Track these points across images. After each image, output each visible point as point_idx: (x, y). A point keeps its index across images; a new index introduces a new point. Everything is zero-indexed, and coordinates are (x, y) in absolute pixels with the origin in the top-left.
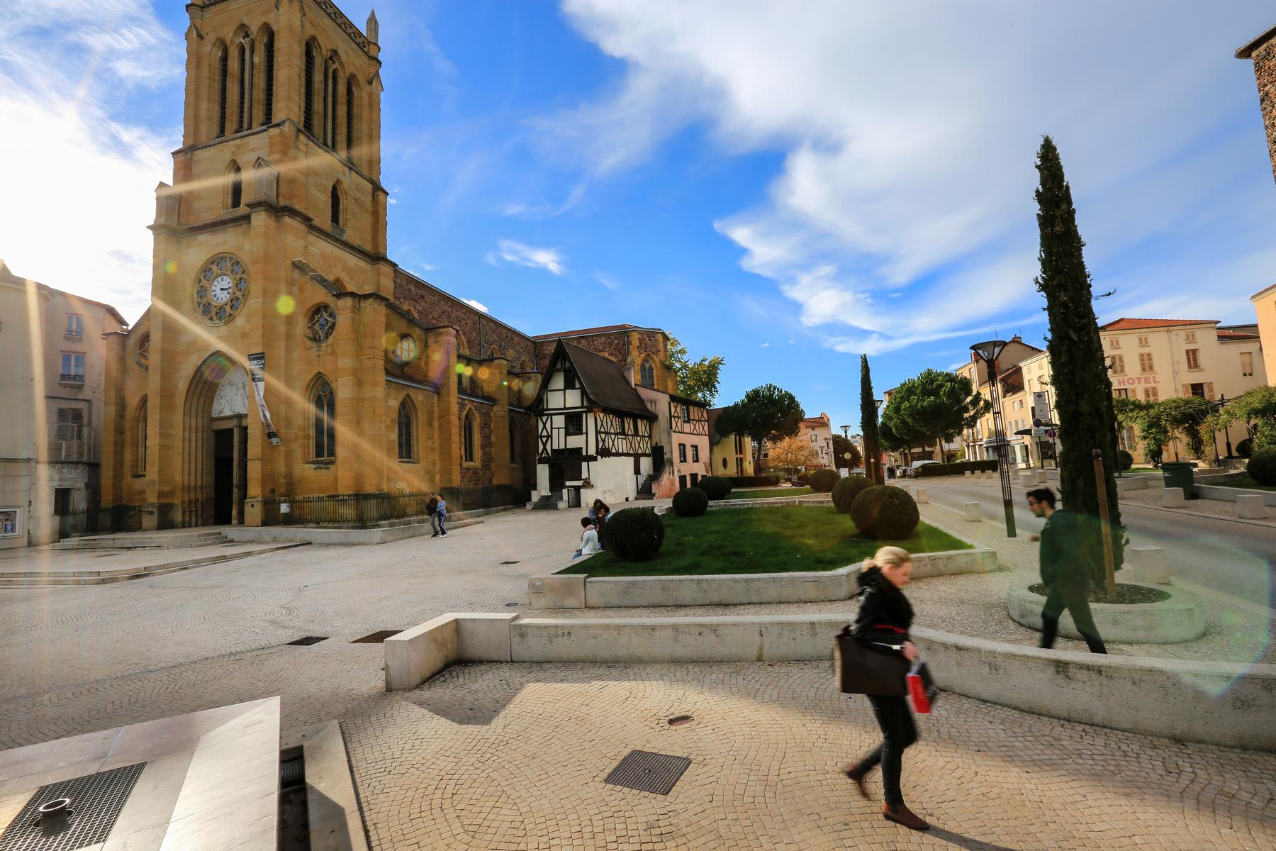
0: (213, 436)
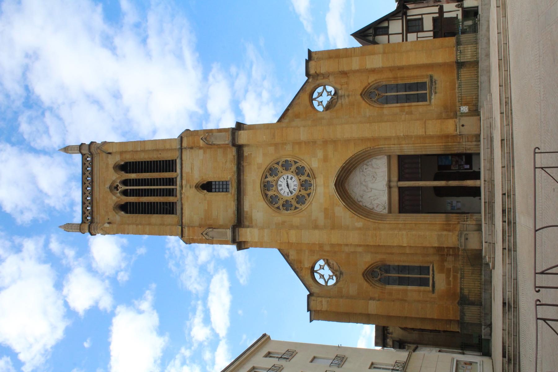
0: (403, 216)
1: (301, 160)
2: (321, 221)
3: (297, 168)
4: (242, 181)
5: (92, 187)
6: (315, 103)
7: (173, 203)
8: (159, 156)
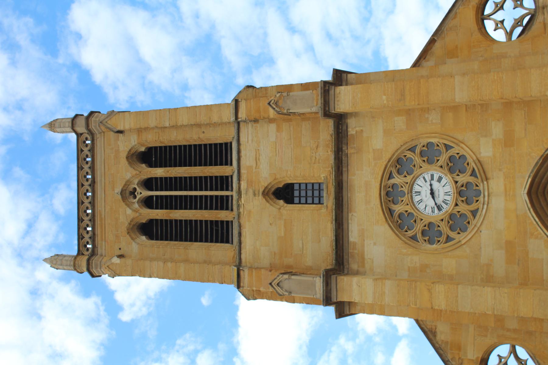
1: (459, 142)
2: (500, 268)
3: (451, 158)
4: (345, 184)
5: (93, 192)
6: (489, 25)
7: (227, 222)
8: (202, 136)
